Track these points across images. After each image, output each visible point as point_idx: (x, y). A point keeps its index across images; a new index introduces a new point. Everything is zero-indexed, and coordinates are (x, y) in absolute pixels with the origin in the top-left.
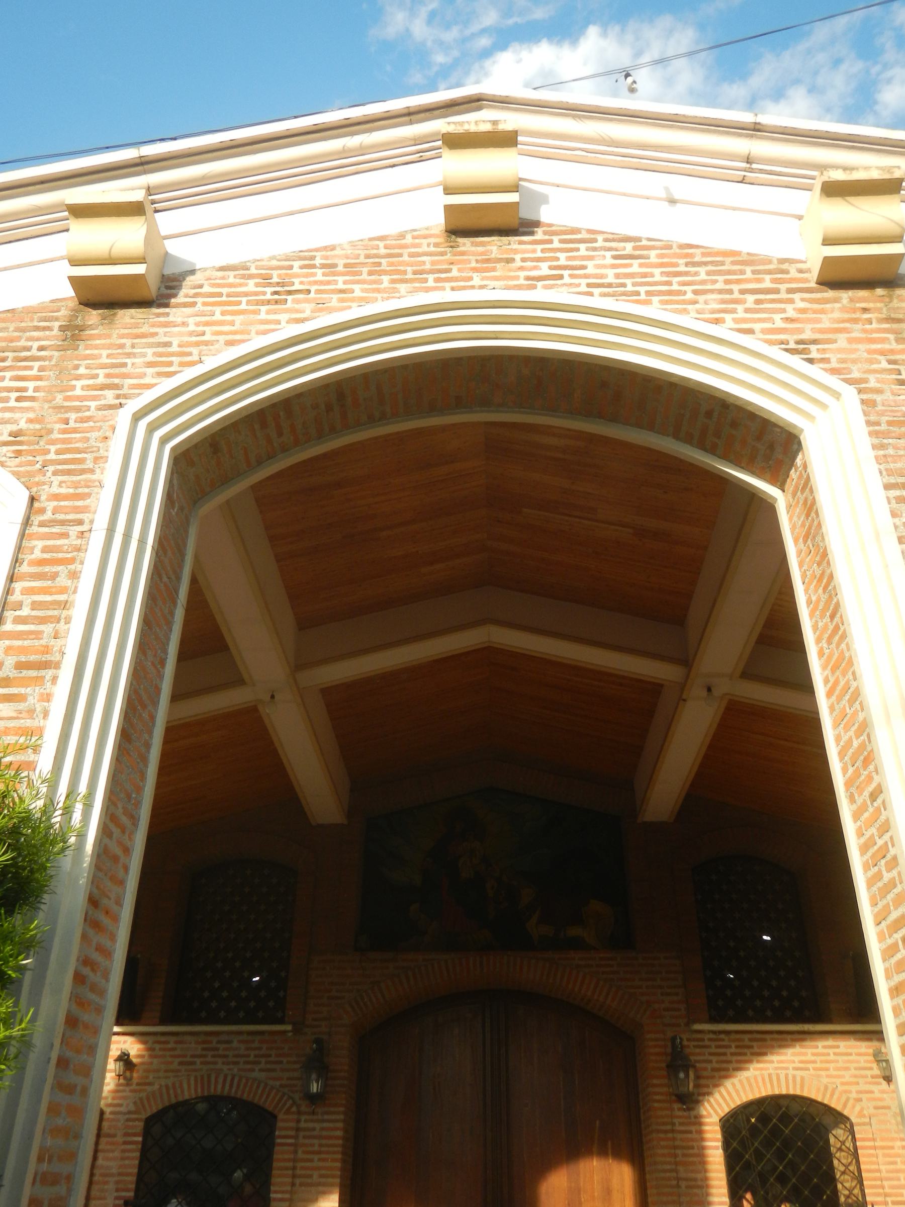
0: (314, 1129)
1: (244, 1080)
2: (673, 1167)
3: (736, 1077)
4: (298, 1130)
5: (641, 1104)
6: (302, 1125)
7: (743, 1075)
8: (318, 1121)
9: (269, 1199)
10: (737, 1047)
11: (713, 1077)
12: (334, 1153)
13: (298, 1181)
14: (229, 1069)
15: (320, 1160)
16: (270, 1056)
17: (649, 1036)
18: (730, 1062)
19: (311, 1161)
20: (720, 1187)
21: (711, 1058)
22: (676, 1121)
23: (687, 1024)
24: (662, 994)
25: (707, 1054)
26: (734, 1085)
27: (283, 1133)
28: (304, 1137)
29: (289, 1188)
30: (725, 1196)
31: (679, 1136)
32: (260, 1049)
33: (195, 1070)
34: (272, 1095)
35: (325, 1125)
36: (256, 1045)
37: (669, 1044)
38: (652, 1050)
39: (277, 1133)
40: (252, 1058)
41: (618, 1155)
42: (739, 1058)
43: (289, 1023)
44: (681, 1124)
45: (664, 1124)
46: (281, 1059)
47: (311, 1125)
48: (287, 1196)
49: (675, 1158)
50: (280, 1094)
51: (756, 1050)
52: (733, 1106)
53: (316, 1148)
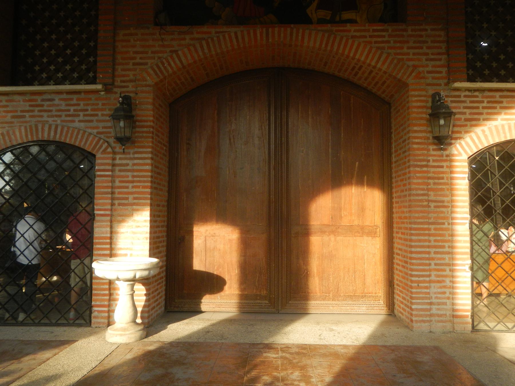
0: (128, 165)
1: (66, 129)
2: (426, 192)
3: (486, 125)
4: (114, 165)
5: (393, 150)
6: (118, 162)
7: (492, 124)
8: (131, 159)
9: (94, 214)
10: (488, 102)
11: (466, 126)
12: (144, 182)
13: (116, 202)
14: (54, 121)
15: (133, 187)
16: (87, 110)
17: (413, 93)
18: (481, 114)
19: (127, 187)
20: (463, 207)
21: (465, 110)
22: (430, 158)
23: (447, 84)
24: (427, 60)
25: (462, 107)
26: (483, 131)
27: (102, 167)
28: (120, 171)
29: (109, 207)
31: (432, 170)
32: (79, 105)
33: (26, 122)
34: (90, 139)
35: (136, 161)
36: (75, 102)
37: (430, 100)
38: (415, 104)
39: (97, 168)
41: (371, 184)
42: (489, 111)
43: (100, 83)
44: (434, 161)
45: (420, 161)
47: (124, 162)
48: (108, 212)
49: (428, 186)
50: (97, 139)
51: (505, 104)
52: (481, 148)
53: (130, 179)
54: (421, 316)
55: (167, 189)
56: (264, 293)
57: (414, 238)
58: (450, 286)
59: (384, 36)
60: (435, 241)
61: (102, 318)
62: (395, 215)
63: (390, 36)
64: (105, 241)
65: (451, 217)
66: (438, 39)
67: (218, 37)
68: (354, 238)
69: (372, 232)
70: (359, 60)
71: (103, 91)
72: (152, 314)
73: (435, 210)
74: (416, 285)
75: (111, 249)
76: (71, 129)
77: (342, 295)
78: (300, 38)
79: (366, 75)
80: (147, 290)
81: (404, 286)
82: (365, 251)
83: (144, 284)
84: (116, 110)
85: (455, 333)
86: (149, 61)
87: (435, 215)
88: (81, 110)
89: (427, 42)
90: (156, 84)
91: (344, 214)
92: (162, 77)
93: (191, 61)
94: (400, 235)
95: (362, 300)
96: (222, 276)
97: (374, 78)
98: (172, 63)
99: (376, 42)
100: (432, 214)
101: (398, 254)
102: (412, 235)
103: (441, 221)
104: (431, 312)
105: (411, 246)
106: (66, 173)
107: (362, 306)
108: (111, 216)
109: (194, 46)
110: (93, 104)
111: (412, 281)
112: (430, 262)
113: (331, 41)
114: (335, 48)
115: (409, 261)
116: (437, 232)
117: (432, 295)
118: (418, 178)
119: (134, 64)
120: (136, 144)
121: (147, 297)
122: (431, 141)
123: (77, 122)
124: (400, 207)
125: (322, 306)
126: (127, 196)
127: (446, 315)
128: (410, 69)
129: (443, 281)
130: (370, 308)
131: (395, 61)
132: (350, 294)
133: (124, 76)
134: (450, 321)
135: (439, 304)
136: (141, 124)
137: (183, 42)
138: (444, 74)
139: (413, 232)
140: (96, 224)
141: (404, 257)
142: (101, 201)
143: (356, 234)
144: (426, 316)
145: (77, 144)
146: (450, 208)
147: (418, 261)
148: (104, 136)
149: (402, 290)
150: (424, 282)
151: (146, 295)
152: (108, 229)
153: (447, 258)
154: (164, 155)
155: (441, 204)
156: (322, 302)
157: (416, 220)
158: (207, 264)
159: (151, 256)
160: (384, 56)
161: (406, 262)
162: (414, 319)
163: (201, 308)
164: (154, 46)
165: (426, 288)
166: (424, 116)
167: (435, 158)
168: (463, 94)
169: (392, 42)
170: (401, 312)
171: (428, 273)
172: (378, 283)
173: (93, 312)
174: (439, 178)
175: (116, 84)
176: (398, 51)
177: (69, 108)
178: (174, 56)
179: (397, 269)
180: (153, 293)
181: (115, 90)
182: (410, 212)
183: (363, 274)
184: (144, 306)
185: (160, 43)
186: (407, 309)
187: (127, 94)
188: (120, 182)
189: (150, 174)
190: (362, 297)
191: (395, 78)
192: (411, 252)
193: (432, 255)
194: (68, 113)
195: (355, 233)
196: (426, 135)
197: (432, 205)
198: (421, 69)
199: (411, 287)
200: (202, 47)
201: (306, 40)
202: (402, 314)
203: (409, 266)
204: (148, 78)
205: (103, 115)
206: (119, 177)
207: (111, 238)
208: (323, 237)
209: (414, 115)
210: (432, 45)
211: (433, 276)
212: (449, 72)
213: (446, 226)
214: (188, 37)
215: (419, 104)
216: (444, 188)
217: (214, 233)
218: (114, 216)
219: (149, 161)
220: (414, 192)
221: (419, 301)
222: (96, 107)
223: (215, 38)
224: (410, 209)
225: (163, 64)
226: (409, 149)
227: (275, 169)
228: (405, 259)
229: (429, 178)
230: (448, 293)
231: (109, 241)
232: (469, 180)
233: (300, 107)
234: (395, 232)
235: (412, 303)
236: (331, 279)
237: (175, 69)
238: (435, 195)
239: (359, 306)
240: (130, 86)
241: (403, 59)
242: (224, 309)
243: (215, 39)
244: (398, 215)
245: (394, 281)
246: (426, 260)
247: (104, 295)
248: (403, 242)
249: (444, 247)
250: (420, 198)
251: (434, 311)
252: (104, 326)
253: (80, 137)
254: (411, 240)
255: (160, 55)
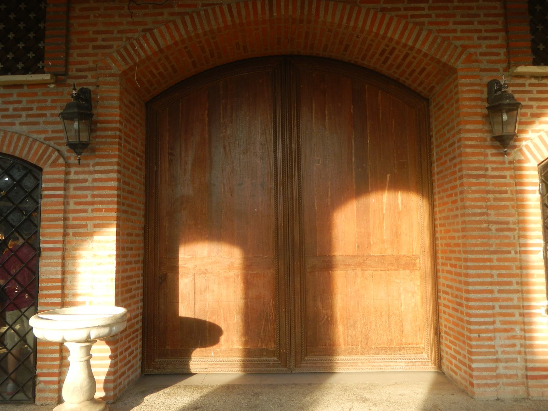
0: (86, 181)
2: (484, 211)
4: (67, 182)
5: (435, 158)
6: (72, 177)
8: (91, 173)
9: (40, 248)
12: (109, 203)
15: (93, 210)
16: (31, 109)
17: (463, 81)
19: (85, 211)
21: (531, 103)
22: (489, 166)
23: (506, 69)
24: (479, 38)
25: (527, 99)
28: (76, 189)
29: (61, 238)
30: (539, 238)
31: (492, 181)
32: (20, 102)
34: (35, 147)
35: (97, 176)
36: (15, 98)
37: (485, 89)
38: (466, 96)
39: (43, 185)
40: (11, 112)
43: (48, 73)
44: (494, 169)
46: (44, 112)
47: (81, 177)
50: (43, 147)
53: (89, 199)
54: (485, 378)
55: (142, 213)
56: (272, 346)
57: (471, 272)
58: (521, 336)
59: (423, 9)
60: (499, 275)
61: (51, 391)
62: (439, 242)
63: (430, 8)
64: (54, 284)
65: (519, 244)
66: (494, 12)
67: (206, 11)
68: (388, 272)
69: (410, 264)
70: (391, 39)
71: (53, 83)
72: (120, 384)
73: (498, 235)
74: (476, 335)
75: (63, 295)
76: (9, 134)
77: (373, 348)
78: (314, 10)
79: (399, 61)
80: (112, 351)
81: (457, 335)
82: (402, 289)
83: (108, 343)
84: (69, 106)
85: (530, 399)
86: (115, 44)
87: (498, 241)
88: (23, 109)
89: (479, 16)
90: (125, 73)
91: (373, 241)
92: (131, 63)
93: (170, 42)
94: (449, 268)
95: (399, 353)
96: (217, 323)
97: (410, 64)
98: (145, 45)
99: (412, 16)
100: (494, 240)
101: (446, 293)
102: (467, 268)
103: (505, 249)
104: (498, 372)
105: (467, 284)
106: (2, 193)
107: (400, 361)
108: (63, 251)
109: (174, 22)
110: (39, 101)
111: (470, 331)
112: (494, 303)
113: (354, 16)
114: (360, 24)
115: (465, 303)
116: (501, 264)
117: (497, 348)
118: (474, 192)
119: (94, 47)
120: (97, 153)
121: (113, 361)
122: (488, 143)
123: (17, 124)
124: (448, 231)
125: (348, 363)
126: (85, 223)
127: (517, 375)
128: (459, 50)
129: (512, 330)
130: (411, 364)
131: (439, 40)
132: (384, 346)
133: (81, 63)
134: (523, 384)
135: (507, 361)
136: (104, 125)
137: (160, 18)
138: (502, 57)
139: (469, 264)
140: (42, 262)
141: (457, 296)
142: (49, 230)
143: (389, 267)
144: (492, 377)
145: (17, 154)
146: (517, 231)
147: (478, 304)
148: (54, 143)
149: (454, 340)
150: (487, 331)
151: (110, 357)
152: (59, 269)
153: (516, 299)
154: (137, 168)
155: (505, 226)
156: (348, 357)
157: (473, 248)
158: (196, 310)
159: (117, 304)
160: (424, 33)
161: (460, 305)
162: (475, 382)
163: (189, 369)
164: (121, 24)
165: (490, 339)
166: (479, 110)
167: (495, 166)
168: (528, 82)
169: (433, 15)
170: (452, 370)
171: (491, 319)
172: (419, 330)
173: (37, 383)
174: (501, 192)
175: (70, 73)
176: (442, 27)
177: (8, 107)
178: (148, 35)
179: (445, 312)
180: (121, 353)
181: (70, 81)
182: (464, 237)
183: (400, 319)
184: (109, 374)
185: (130, 19)
186: (463, 367)
187: (84, 87)
188: (76, 203)
189: (115, 192)
190: (400, 349)
191: (439, 62)
192: (468, 291)
193: (496, 295)
194: (6, 113)
195: (388, 265)
196: (482, 135)
197: (493, 227)
198: (472, 50)
199: (470, 339)
200: (184, 24)
201: (322, 15)
202: (456, 373)
203: (464, 309)
204: (113, 65)
205: (52, 115)
206: (74, 197)
207: (63, 280)
208: (347, 271)
209: (465, 110)
210: (486, 19)
211: (497, 322)
212: (508, 53)
213: (512, 255)
214: (166, 11)
215: (471, 95)
216: (508, 206)
217: (206, 270)
218: (67, 250)
219: (115, 175)
220: (469, 211)
221: (480, 357)
222: (43, 105)
223: (201, 12)
224: (464, 233)
225: (133, 47)
226: (460, 155)
227: (283, 184)
228: (458, 300)
229: (488, 192)
230: (518, 345)
231: (59, 284)
232: (540, 194)
233: (314, 105)
234: (440, 264)
235: (471, 361)
236: (359, 326)
237: (149, 53)
238: (497, 215)
239: (396, 362)
240: (90, 77)
241: (448, 38)
242: (219, 369)
243: (202, 13)
244: (444, 241)
245: (440, 327)
246: (489, 302)
247: (54, 359)
248: (453, 277)
249: (510, 283)
250: (478, 218)
251: (501, 371)
252: (53, 403)
253: (20, 144)
254: (467, 275)
255: (130, 35)
